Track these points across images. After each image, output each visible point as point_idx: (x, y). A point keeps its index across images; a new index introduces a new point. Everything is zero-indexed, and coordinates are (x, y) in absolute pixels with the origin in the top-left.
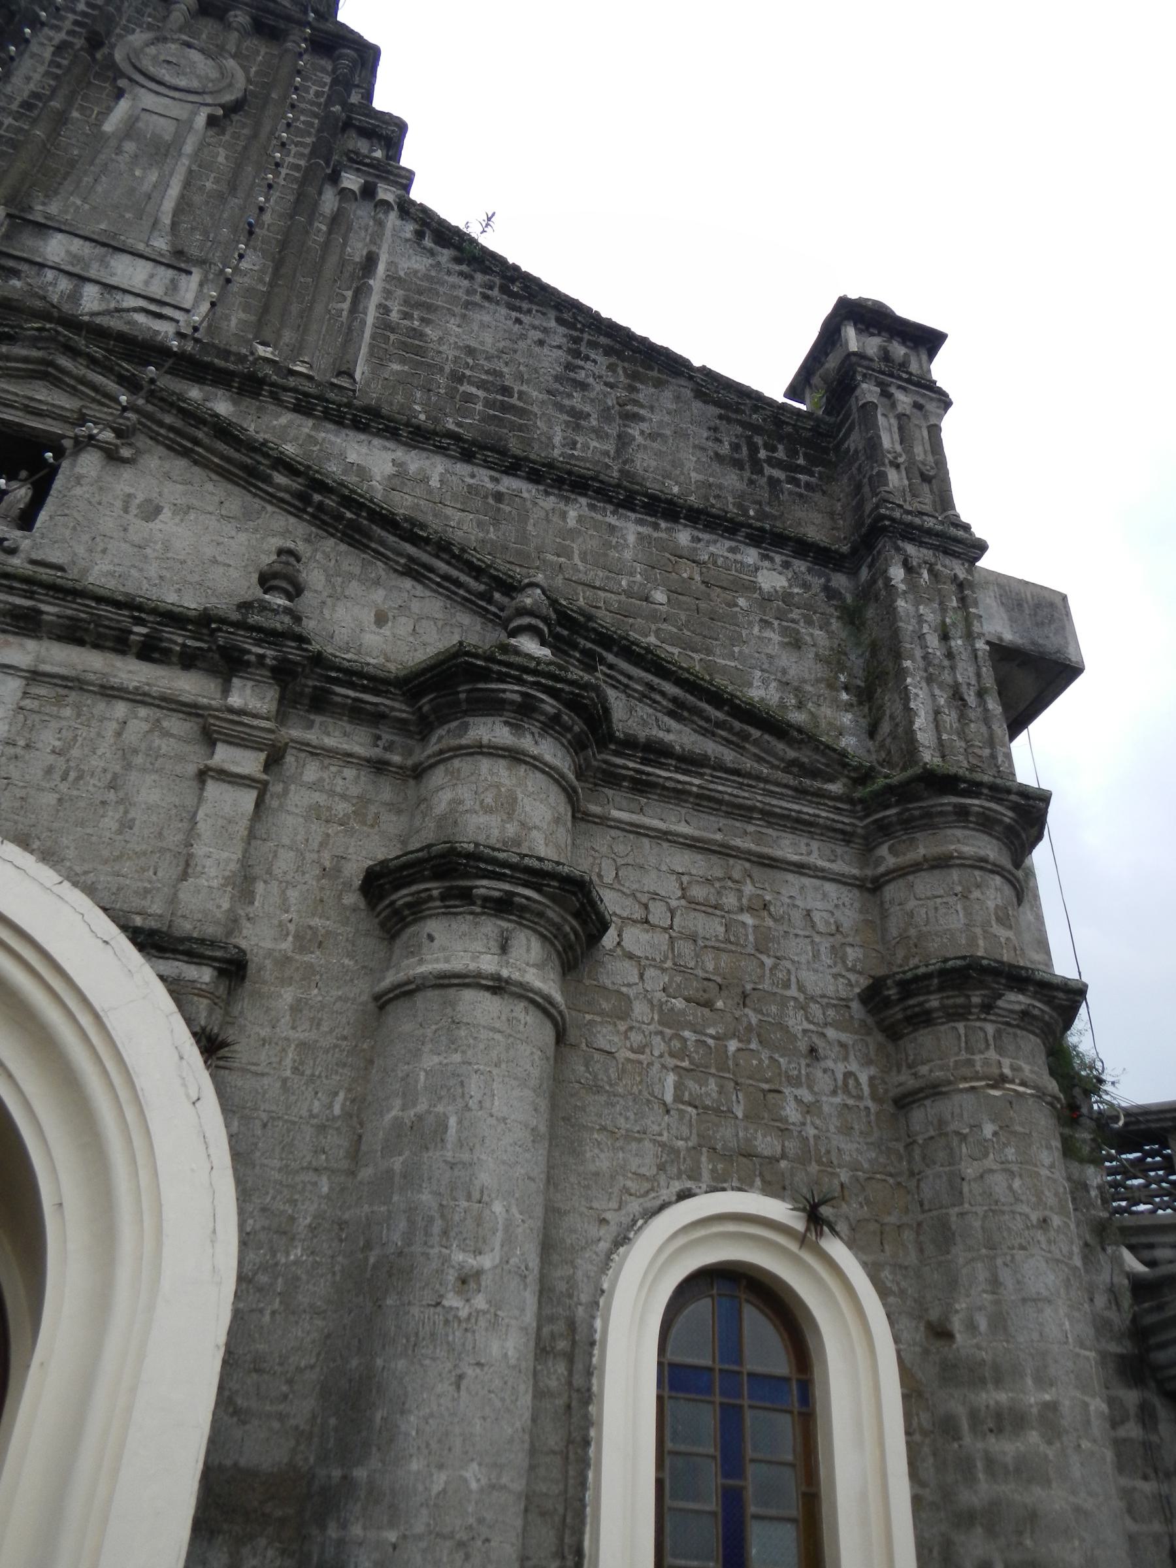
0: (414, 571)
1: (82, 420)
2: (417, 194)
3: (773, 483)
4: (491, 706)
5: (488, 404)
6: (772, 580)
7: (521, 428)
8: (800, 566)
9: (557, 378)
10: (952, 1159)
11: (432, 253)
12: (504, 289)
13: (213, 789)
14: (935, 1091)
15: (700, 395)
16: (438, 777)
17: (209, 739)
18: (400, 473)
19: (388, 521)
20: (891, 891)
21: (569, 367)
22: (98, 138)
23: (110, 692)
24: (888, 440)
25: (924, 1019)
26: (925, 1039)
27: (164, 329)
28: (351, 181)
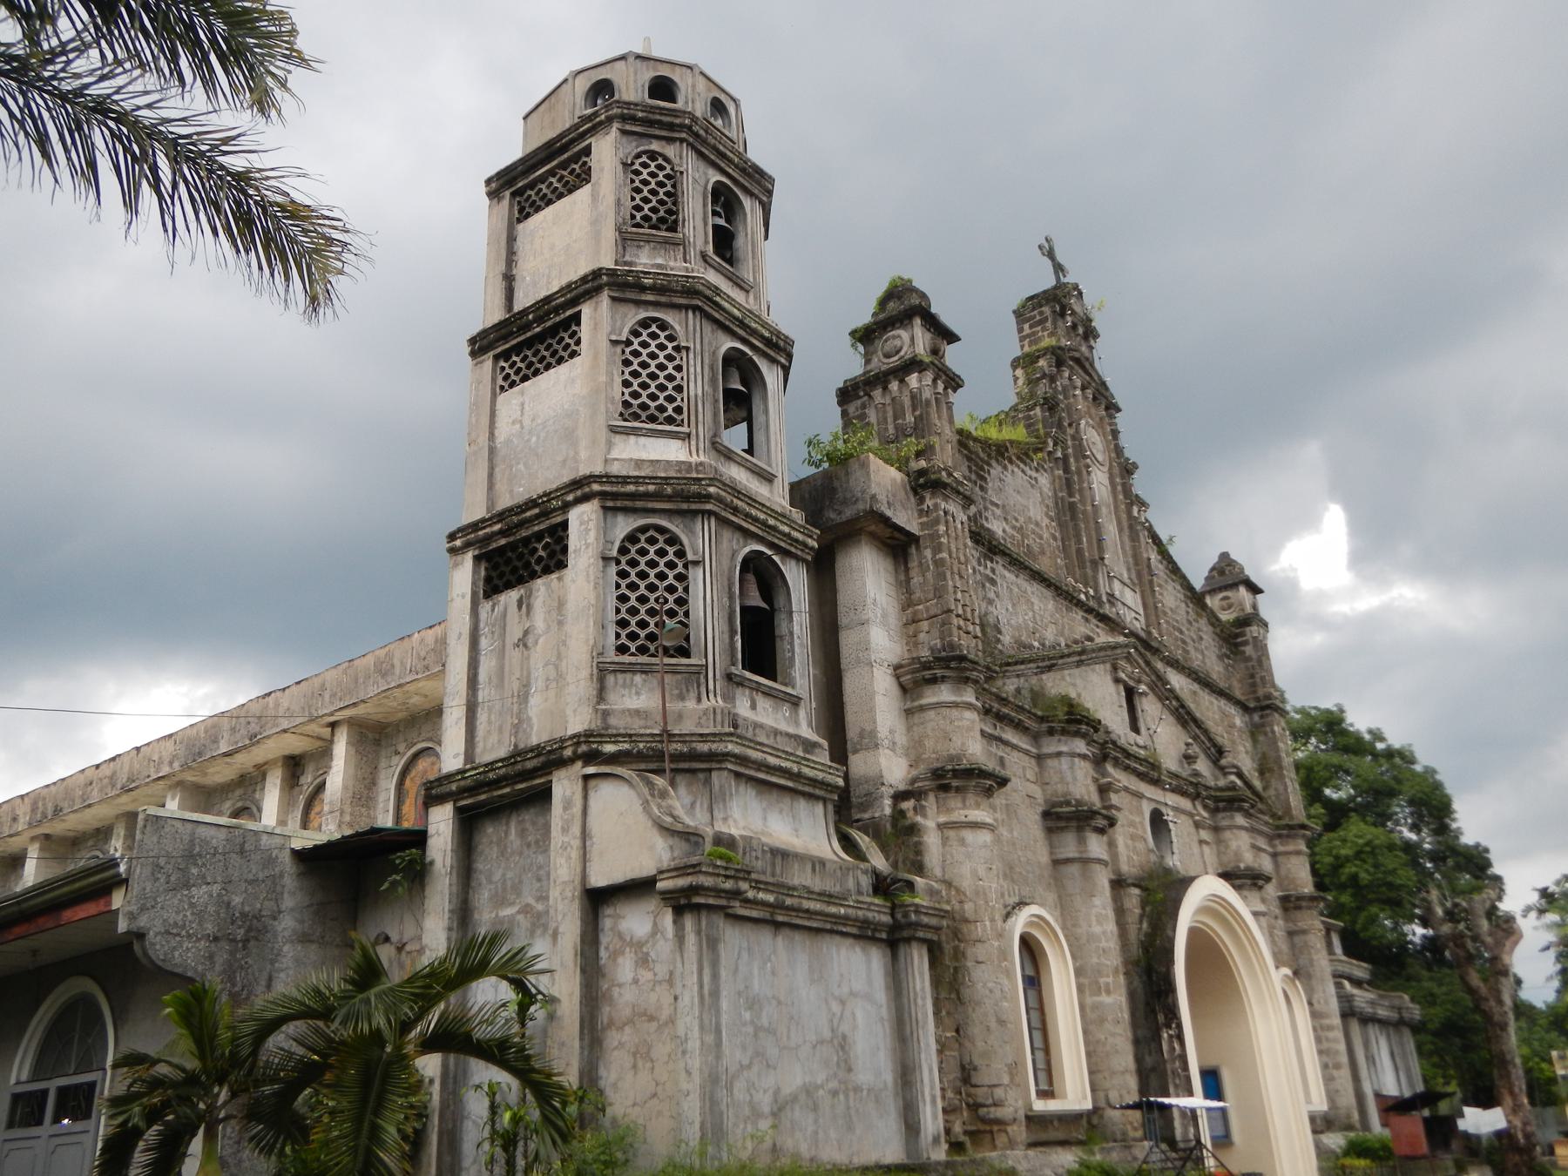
1: (1139, 681)
4: (1240, 809)
6: (1238, 722)
10: (1310, 954)
13: (1204, 846)
14: (1304, 932)
16: (1227, 834)
19: (1195, 721)
20: (1280, 859)
25: (1299, 908)
26: (1298, 914)
27: (1138, 625)
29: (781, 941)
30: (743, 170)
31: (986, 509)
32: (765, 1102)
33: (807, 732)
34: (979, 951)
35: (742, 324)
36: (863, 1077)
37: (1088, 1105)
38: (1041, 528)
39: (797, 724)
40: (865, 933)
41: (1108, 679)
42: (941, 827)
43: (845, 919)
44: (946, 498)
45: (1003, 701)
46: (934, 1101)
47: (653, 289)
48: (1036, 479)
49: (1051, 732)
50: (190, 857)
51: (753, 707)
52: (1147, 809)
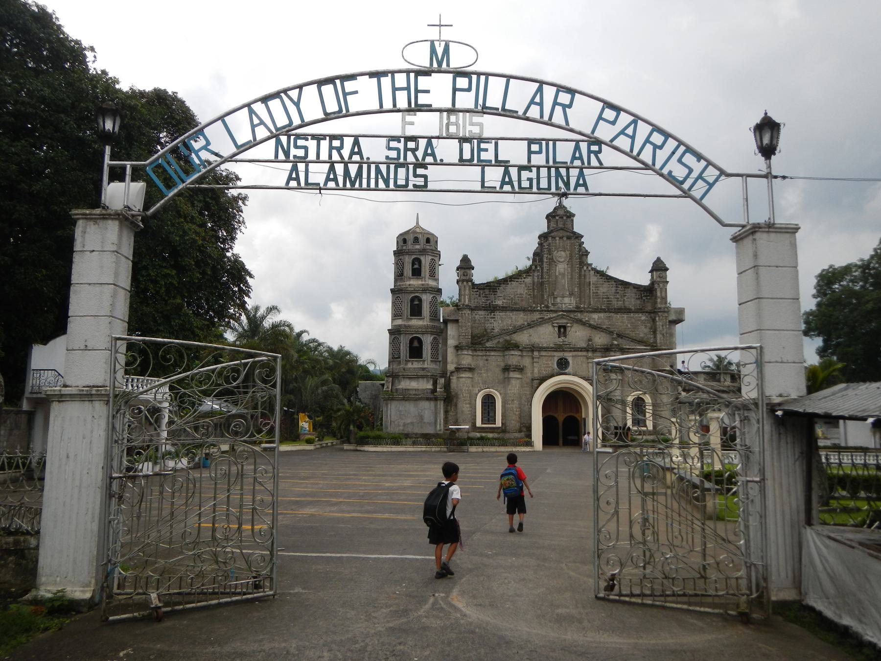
0: (602, 331)
1: (567, 323)
2: (593, 266)
3: (644, 300)
4: (612, 351)
5: (607, 301)
6: (643, 318)
7: (611, 304)
8: (647, 314)
9: (615, 293)
11: (597, 276)
12: (607, 279)
15: (634, 288)
17: (588, 359)
18: (599, 318)
21: (616, 290)
22: (556, 276)
23: (579, 356)
24: (659, 294)
27: (571, 307)
28: (585, 268)
29: (407, 402)
30: (420, 252)
31: (495, 299)
32: (402, 424)
33: (426, 366)
34: (459, 400)
35: (414, 290)
36: (426, 420)
37: (500, 426)
38: (523, 294)
39: (424, 364)
40: (428, 399)
41: (551, 326)
42: (458, 378)
43: (421, 398)
44: (462, 311)
45: (487, 347)
46: (440, 425)
47: (397, 291)
48: (524, 281)
49: (505, 350)
50: (366, 388)
51: (412, 364)
52: (556, 359)
